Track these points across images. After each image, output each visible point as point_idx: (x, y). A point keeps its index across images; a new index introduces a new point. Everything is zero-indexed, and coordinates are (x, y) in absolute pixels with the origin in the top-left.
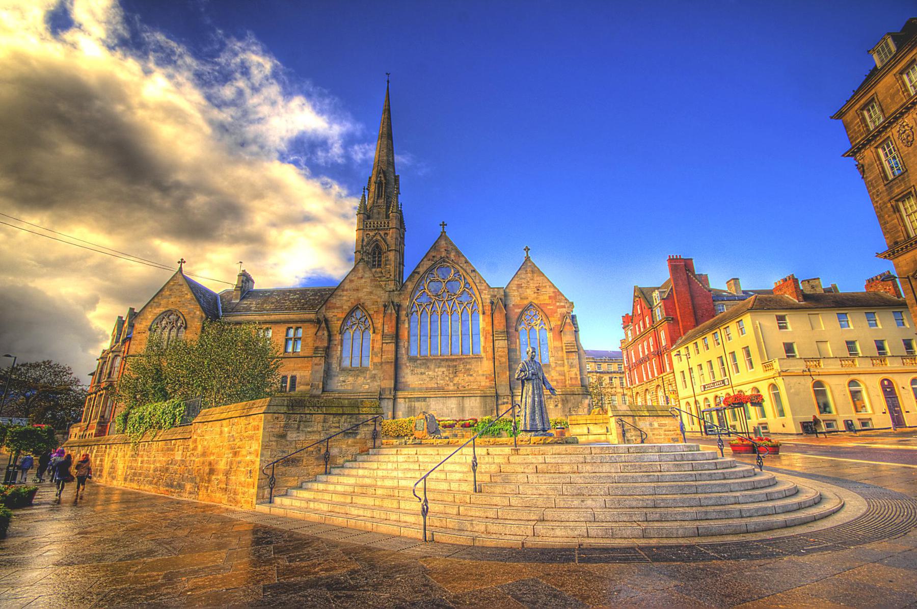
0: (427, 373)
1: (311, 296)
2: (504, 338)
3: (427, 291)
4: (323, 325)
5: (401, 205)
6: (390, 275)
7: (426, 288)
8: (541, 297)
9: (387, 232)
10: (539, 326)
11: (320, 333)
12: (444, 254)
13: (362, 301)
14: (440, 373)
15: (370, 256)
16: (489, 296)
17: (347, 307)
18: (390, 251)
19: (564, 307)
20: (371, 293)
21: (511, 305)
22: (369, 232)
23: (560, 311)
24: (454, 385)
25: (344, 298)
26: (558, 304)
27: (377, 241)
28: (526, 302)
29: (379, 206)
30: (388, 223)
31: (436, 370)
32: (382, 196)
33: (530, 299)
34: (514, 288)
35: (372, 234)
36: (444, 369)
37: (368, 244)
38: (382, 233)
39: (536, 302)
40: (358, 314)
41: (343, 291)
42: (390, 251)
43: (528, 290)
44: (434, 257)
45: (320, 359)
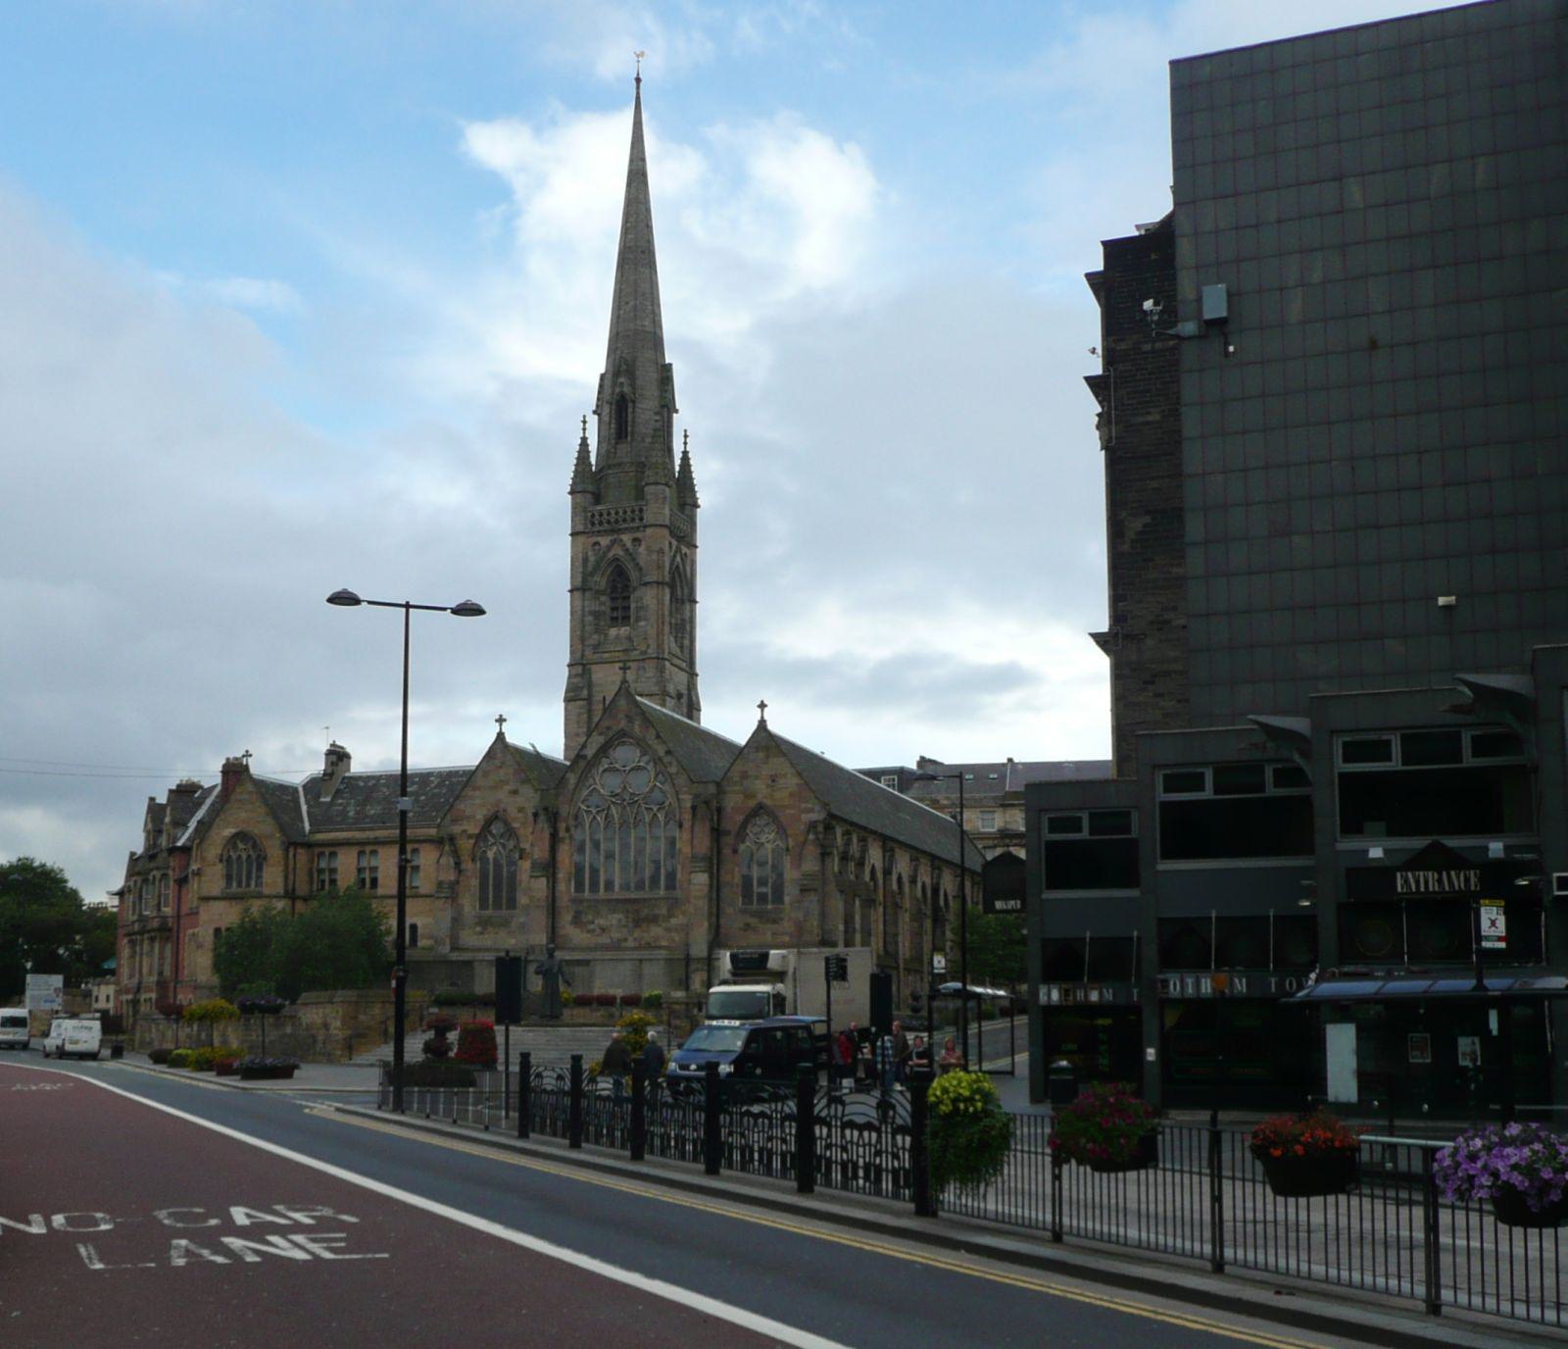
0: (596, 922)
1: (435, 788)
2: (703, 869)
3: (599, 787)
4: (447, 848)
5: (686, 436)
6: (648, 646)
7: (597, 782)
8: (778, 795)
9: (638, 535)
10: (774, 842)
11: (443, 861)
12: (623, 724)
13: (502, 806)
14: (614, 922)
15: (603, 598)
16: (691, 797)
17: (480, 815)
18: (646, 584)
19: (811, 810)
20: (515, 792)
21: (729, 810)
22: (599, 539)
23: (806, 818)
24: (635, 939)
25: (478, 801)
26: (803, 805)
27: (618, 559)
28: (752, 803)
29: (620, 465)
30: (641, 511)
31: (610, 917)
32: (626, 437)
33: (759, 798)
34: (735, 779)
35: (605, 541)
36: (621, 916)
37: (597, 567)
38: (626, 538)
39: (769, 802)
40: (496, 828)
41: (475, 789)
42: (646, 584)
43: (757, 782)
44: (608, 728)
45: (446, 902)
